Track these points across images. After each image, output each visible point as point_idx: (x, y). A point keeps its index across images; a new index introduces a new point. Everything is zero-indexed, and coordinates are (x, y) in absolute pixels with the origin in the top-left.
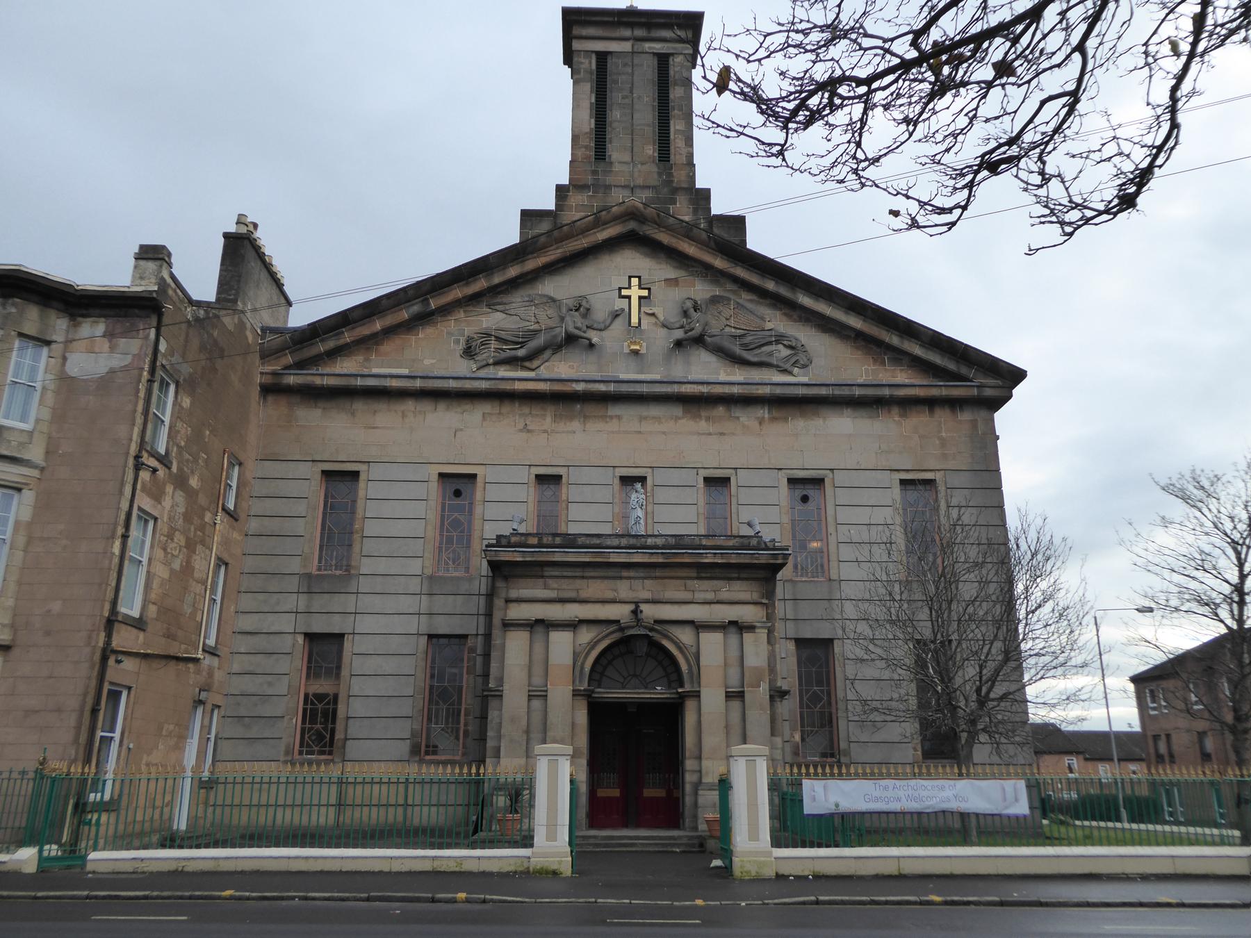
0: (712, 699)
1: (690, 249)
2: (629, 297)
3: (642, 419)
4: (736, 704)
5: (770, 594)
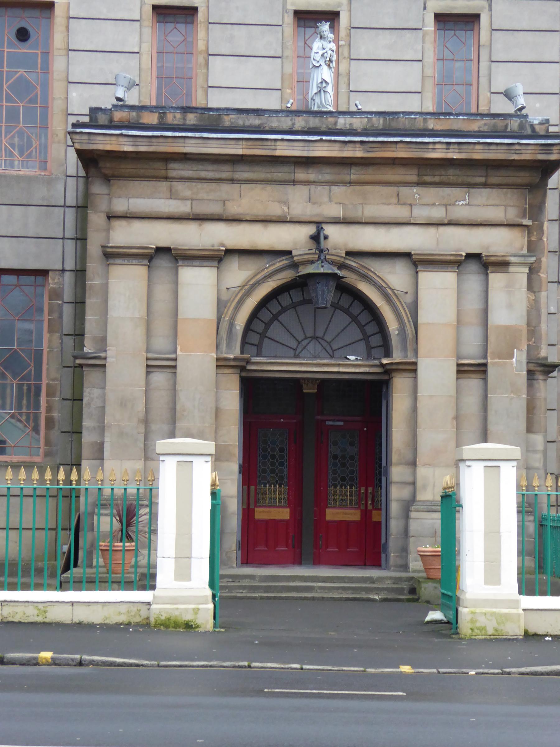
0: (435, 374)
4: (473, 384)
5: (535, 210)
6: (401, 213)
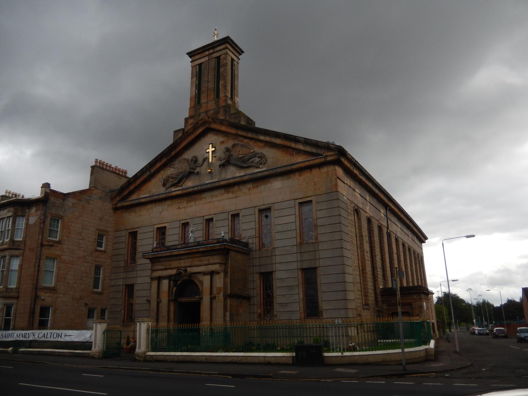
1: (223, 128)
2: (209, 152)
3: (212, 196)
6: (199, 263)
